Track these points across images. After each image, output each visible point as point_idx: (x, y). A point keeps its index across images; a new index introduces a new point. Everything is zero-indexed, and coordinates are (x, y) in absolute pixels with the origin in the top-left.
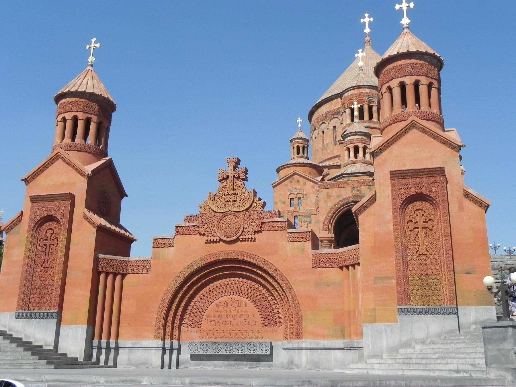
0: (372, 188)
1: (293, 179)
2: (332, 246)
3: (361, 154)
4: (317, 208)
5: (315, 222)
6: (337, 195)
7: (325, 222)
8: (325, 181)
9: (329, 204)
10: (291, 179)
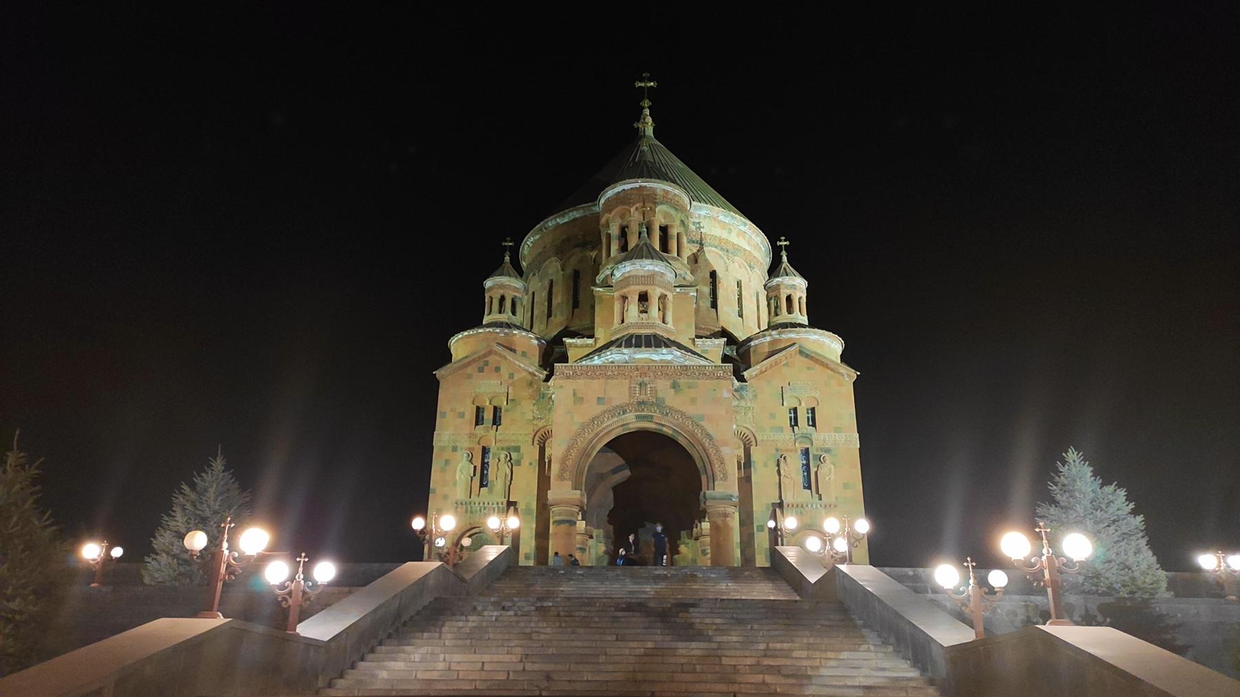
0: (681, 388)
1: (486, 363)
2: (1060, 584)
3: (654, 311)
4: (536, 431)
5: (531, 464)
6: (598, 398)
7: (702, 430)
8: (568, 363)
9: (578, 420)
10: (481, 364)
